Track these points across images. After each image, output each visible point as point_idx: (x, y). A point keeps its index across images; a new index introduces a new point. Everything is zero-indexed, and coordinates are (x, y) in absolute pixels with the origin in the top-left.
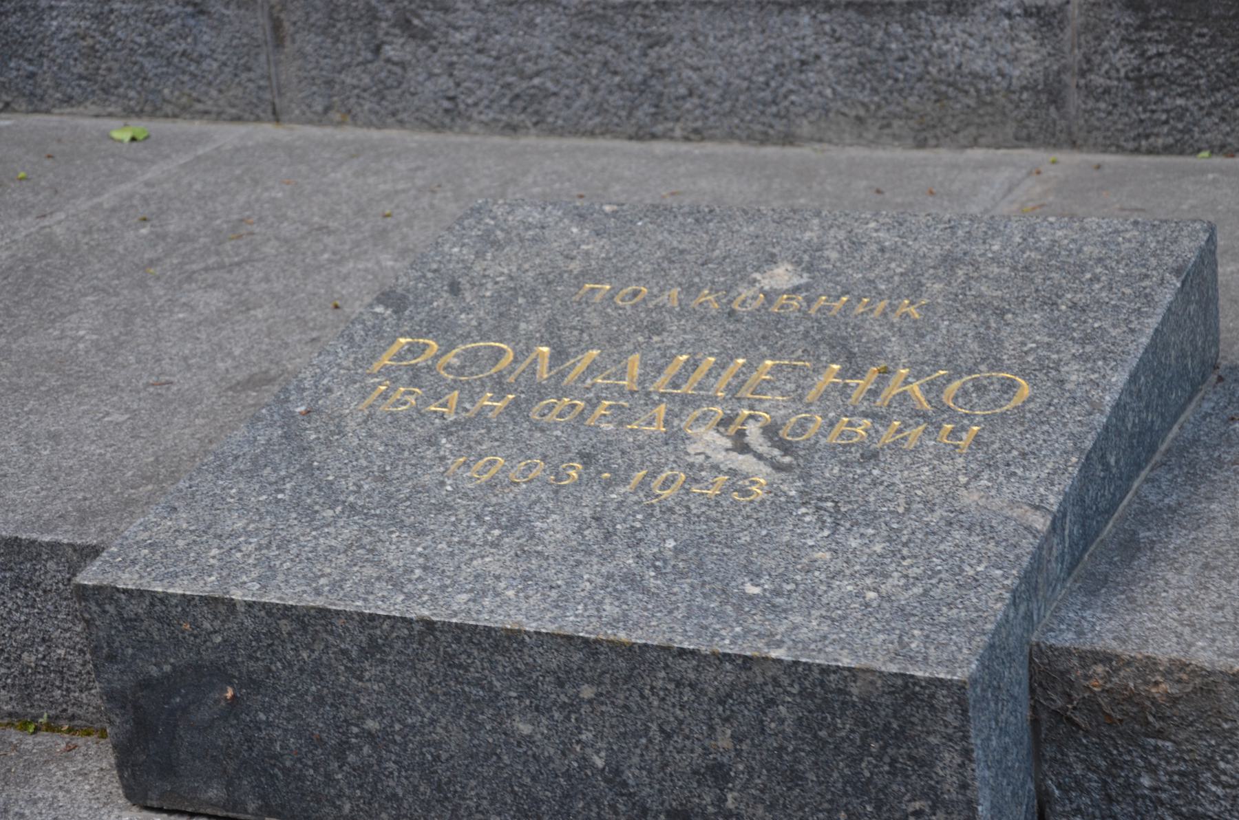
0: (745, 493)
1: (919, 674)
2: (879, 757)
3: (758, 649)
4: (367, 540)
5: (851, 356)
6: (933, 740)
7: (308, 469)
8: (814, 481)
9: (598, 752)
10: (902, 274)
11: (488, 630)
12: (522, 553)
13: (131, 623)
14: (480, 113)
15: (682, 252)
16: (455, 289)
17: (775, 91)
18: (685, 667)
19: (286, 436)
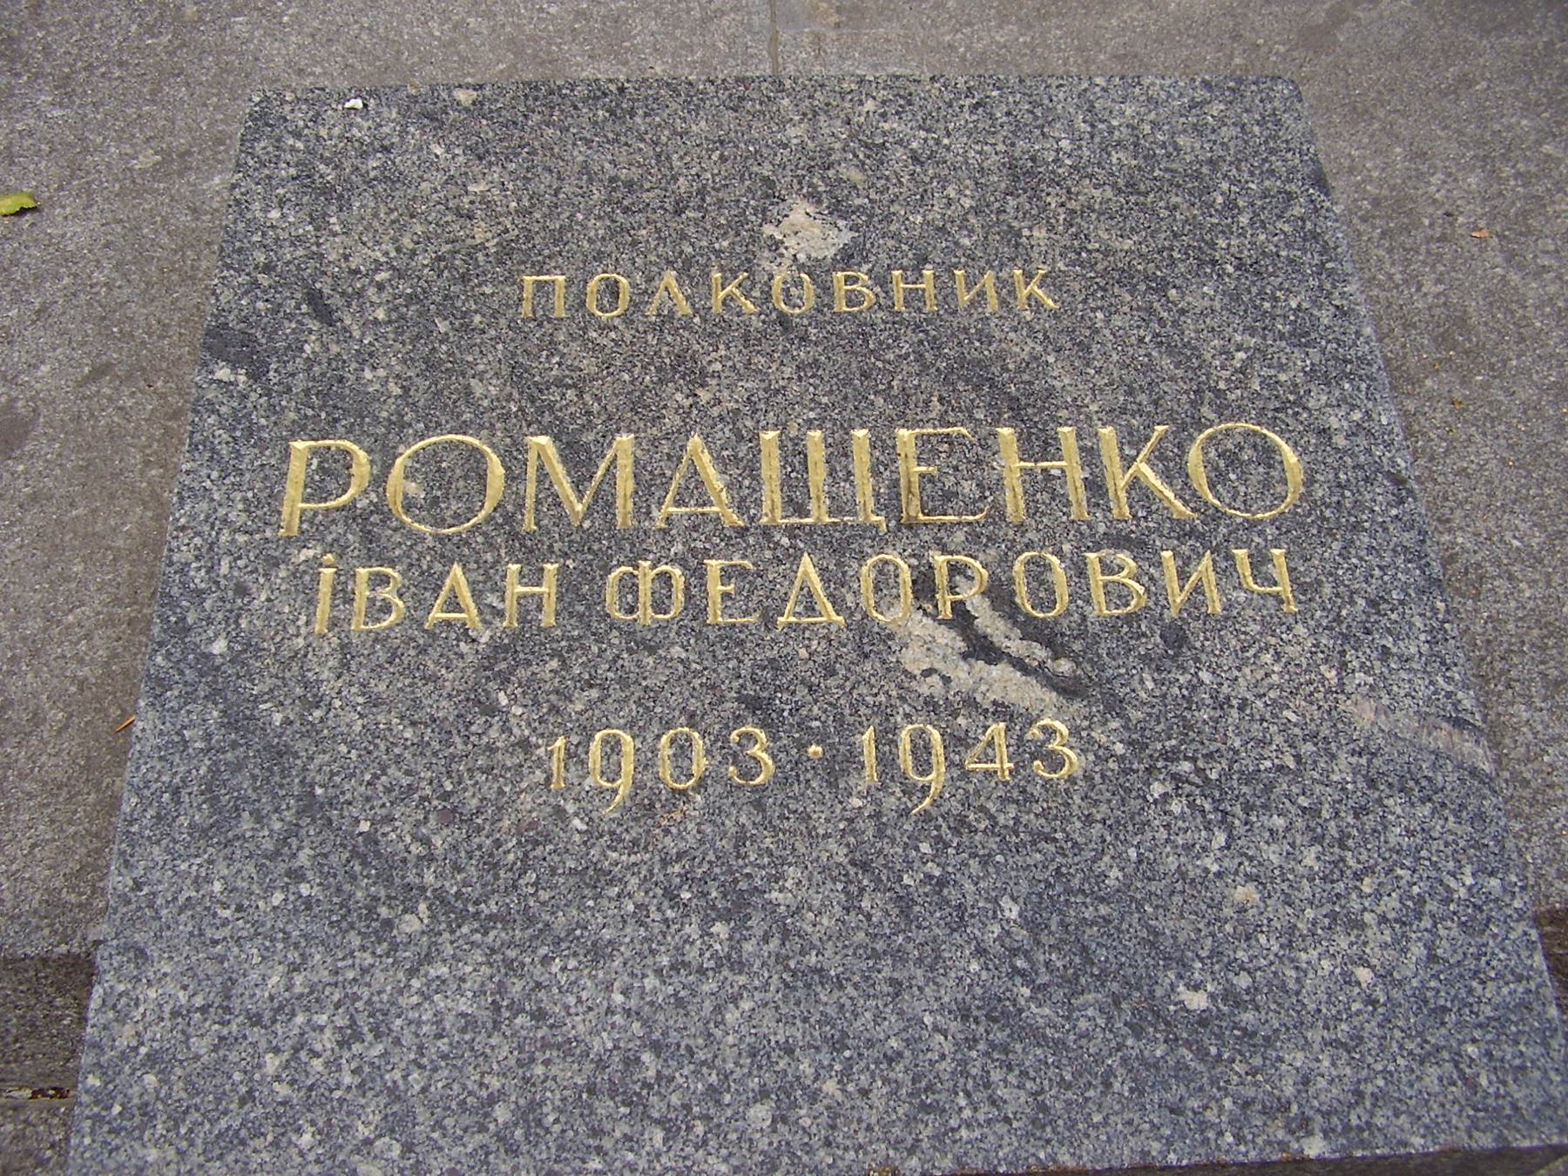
0: (1055, 762)
1: (1526, 1144)
4: (516, 987)
5: (1017, 413)
7: (309, 804)
10: (977, 211)
15: (630, 185)
16: (324, 313)
19: (231, 722)
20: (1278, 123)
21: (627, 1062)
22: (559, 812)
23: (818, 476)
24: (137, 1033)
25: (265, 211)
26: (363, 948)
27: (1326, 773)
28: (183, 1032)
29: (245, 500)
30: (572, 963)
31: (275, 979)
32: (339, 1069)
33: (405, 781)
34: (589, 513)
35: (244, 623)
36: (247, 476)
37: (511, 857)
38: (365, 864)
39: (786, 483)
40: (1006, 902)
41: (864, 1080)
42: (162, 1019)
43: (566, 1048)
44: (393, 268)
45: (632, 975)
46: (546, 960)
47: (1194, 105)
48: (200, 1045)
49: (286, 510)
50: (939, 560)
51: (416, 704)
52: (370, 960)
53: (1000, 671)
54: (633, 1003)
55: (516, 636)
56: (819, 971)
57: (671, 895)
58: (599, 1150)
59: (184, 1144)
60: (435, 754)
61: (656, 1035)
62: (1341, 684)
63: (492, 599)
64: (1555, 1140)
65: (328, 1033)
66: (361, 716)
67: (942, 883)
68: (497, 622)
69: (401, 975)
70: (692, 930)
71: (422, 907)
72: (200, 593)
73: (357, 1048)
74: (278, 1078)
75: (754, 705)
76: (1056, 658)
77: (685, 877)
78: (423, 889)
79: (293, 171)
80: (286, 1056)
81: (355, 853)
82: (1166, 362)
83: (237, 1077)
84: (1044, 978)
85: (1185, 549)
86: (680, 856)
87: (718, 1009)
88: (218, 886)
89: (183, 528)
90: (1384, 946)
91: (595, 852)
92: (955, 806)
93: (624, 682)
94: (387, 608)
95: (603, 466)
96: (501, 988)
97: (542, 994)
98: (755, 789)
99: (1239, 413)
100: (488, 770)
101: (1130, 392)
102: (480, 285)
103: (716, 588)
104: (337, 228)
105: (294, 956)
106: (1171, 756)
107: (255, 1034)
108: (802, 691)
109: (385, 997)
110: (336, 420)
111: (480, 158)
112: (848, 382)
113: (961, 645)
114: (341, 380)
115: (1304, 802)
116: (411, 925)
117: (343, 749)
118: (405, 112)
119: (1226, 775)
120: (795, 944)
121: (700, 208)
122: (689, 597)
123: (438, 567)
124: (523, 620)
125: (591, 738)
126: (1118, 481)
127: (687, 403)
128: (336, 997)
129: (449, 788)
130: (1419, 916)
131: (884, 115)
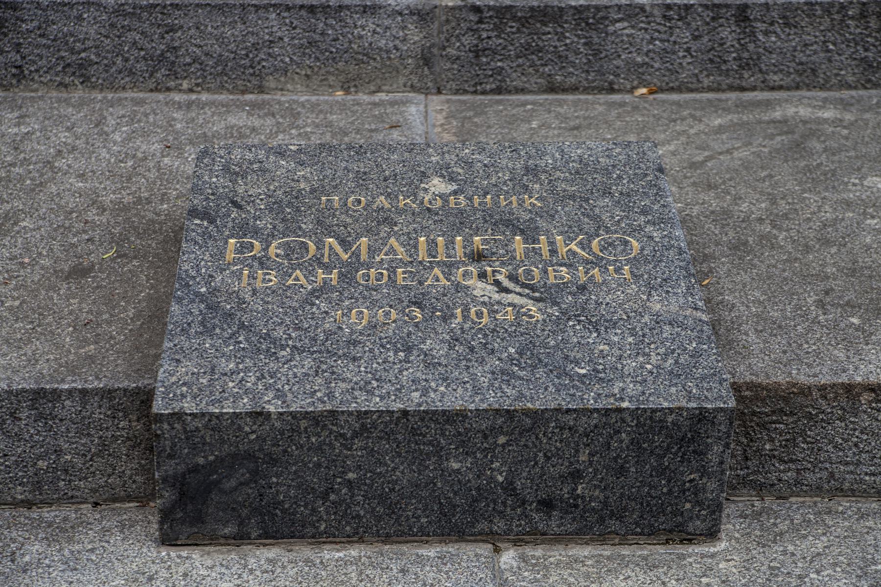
2: (676, 454)
3: (612, 404)
4: (324, 367)
5: (522, 232)
6: (709, 440)
7: (242, 326)
8: (563, 306)
9: (501, 474)
11: (444, 412)
13: (189, 435)
14: (40, 76)
15: (365, 173)
16: (239, 207)
17: (252, 60)
18: (570, 420)
19: (209, 307)
20: (645, 154)
21: (366, 383)
23: (441, 249)
25: (210, 178)
34: (350, 257)
35: (213, 284)
41: (455, 387)
43: (344, 380)
47: (608, 149)
57: (383, 346)
58: (356, 402)
62: (648, 300)
64: (722, 406)
67: (486, 344)
70: (391, 354)
72: (194, 278)
75: (415, 303)
77: (388, 342)
81: (261, 337)
82: (586, 220)
85: (588, 267)
86: (386, 338)
88: (207, 345)
91: (354, 337)
92: (492, 327)
93: (364, 298)
94: (271, 281)
95: (355, 246)
99: (616, 232)
100: (312, 318)
106: (579, 315)
108: (433, 300)
116: (283, 353)
123: (290, 271)
124: (325, 283)
130: (673, 354)
131: (473, 154)
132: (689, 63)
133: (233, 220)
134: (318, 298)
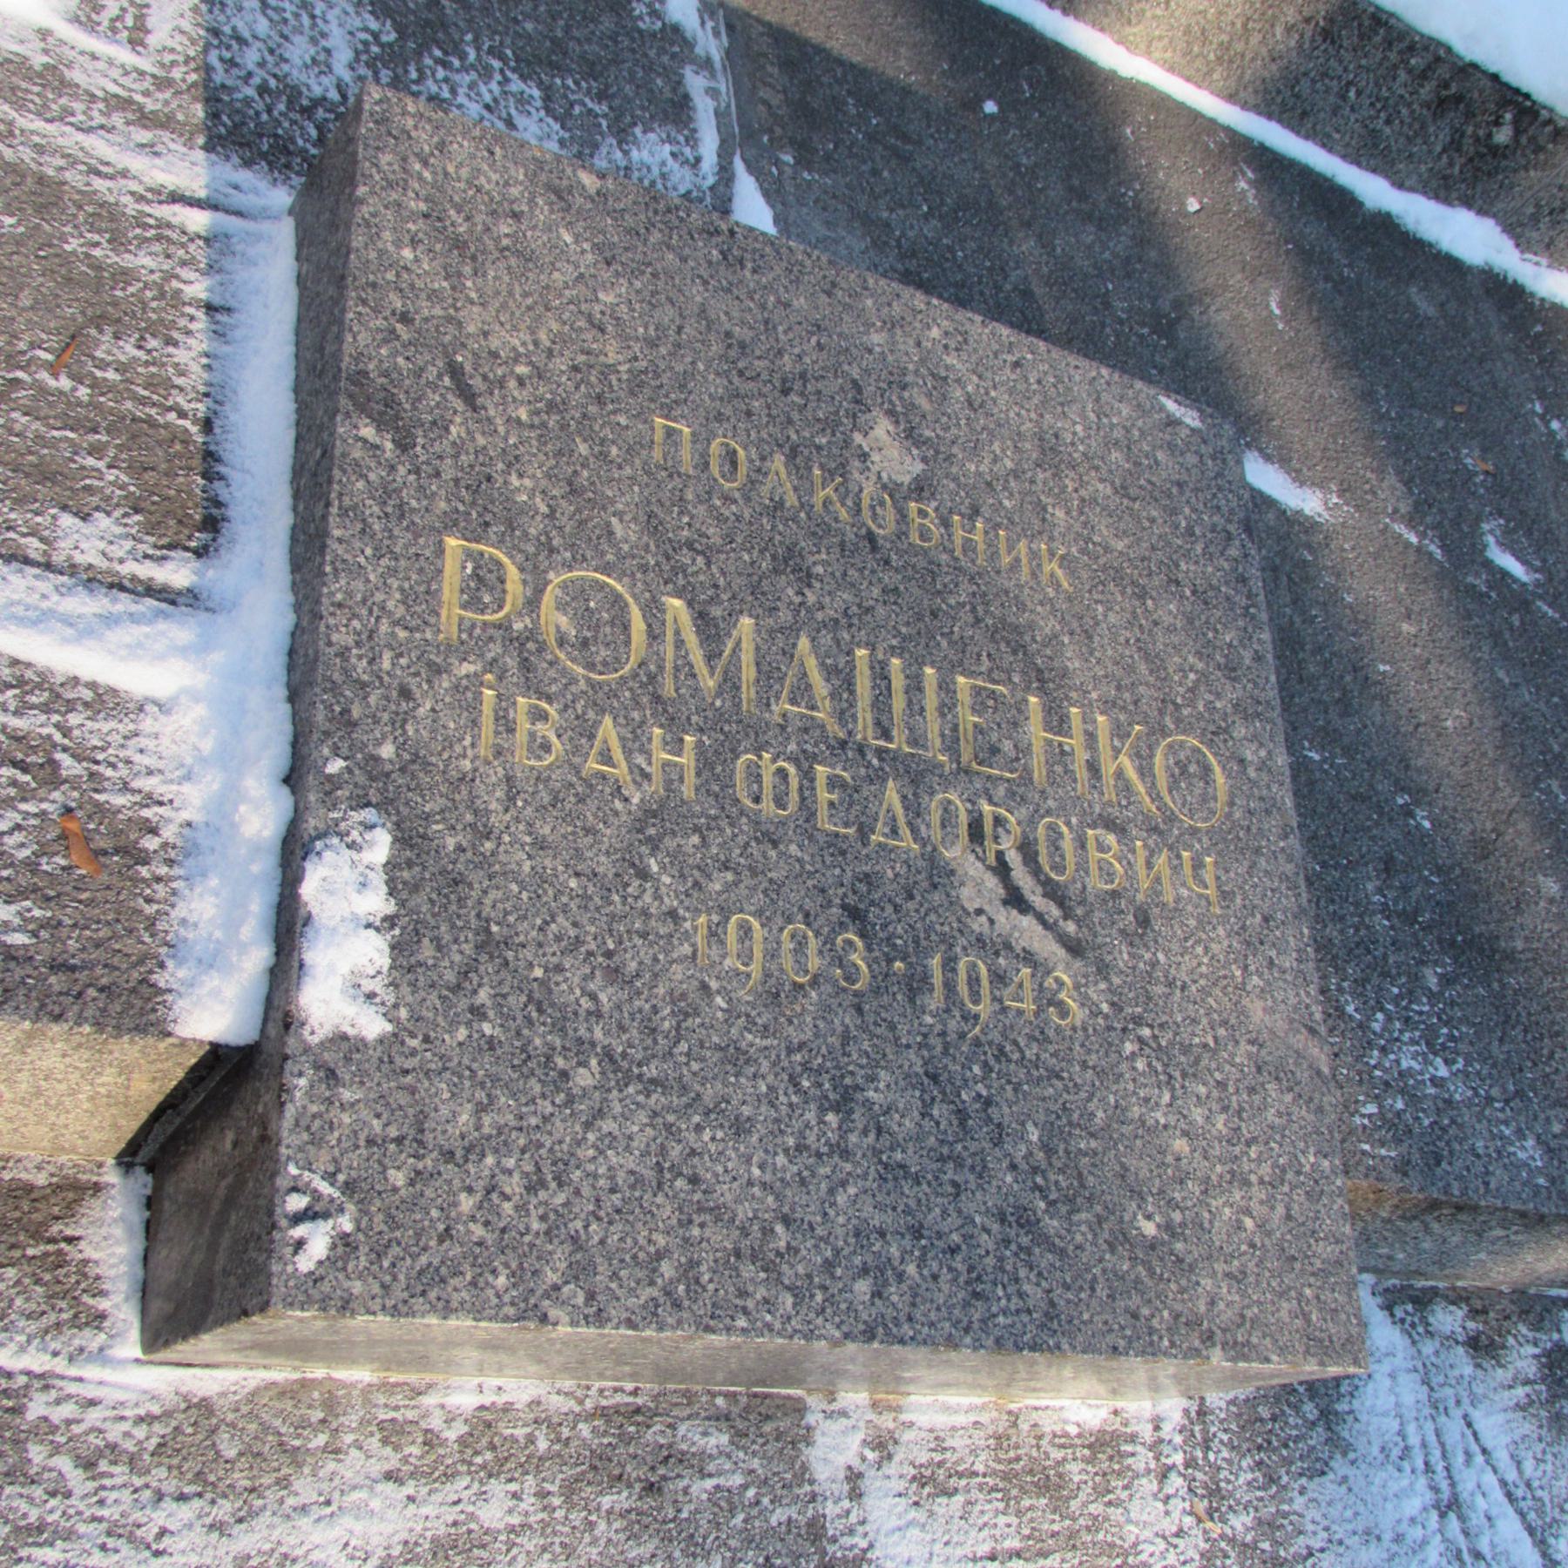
7: (487, 943)
12: (893, 1173)
21: (764, 1230)
22: (704, 987)
23: (898, 703)
24: (335, 1160)
25: (398, 244)
26: (544, 1096)
27: (1232, 1055)
28: (380, 1162)
29: (402, 590)
30: (720, 1135)
31: (465, 1117)
32: (528, 1215)
33: (572, 932)
36: (403, 563)
37: (667, 1024)
38: (540, 1011)
39: (875, 704)
40: (1030, 1127)
42: (357, 1147)
43: (718, 1213)
44: (530, 363)
45: (766, 1151)
46: (699, 1128)
48: (398, 1178)
49: (444, 613)
50: (987, 808)
51: (578, 854)
52: (550, 1109)
53: (1027, 921)
54: (768, 1178)
55: (662, 804)
56: (902, 1166)
58: (745, 1311)
59: (388, 1278)
60: (597, 909)
61: (786, 1209)
63: (640, 760)
65: (516, 1177)
66: (530, 857)
67: (988, 1102)
68: (645, 785)
69: (578, 1128)
70: (811, 1116)
71: (594, 1062)
73: (542, 1195)
74: (473, 1218)
75: (855, 914)
76: (1065, 918)
77: (805, 1066)
78: (593, 1044)
79: (423, 206)
80: (479, 1196)
81: (530, 999)
82: (1143, 668)
83: (435, 1213)
84: (1053, 1196)
86: (802, 1045)
87: (831, 1191)
89: (340, 605)
90: (1262, 1202)
92: (995, 1036)
93: (754, 873)
95: (730, 645)
96: (663, 1151)
97: (696, 1160)
98: (856, 994)
100: (644, 935)
101: (1118, 688)
102: (615, 412)
103: (824, 795)
104: (473, 295)
105: (480, 1095)
106: (1138, 1021)
107: (449, 1170)
108: (889, 909)
109: (565, 1147)
110: (487, 524)
111: (608, 264)
112: (920, 617)
113: (1001, 891)
114: (489, 479)
115: (1218, 1076)
116: (583, 1079)
117: (514, 887)
118: (532, 178)
119: (1171, 1043)
120: (886, 1141)
121: (802, 394)
122: (803, 799)
123: (591, 714)
125: (727, 919)
126: (1108, 769)
127: (798, 599)
128: (522, 1142)
129: (611, 946)
130: (1282, 1182)
132: (1154, 17)
133: (458, 448)
134: (654, 844)
